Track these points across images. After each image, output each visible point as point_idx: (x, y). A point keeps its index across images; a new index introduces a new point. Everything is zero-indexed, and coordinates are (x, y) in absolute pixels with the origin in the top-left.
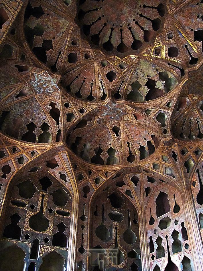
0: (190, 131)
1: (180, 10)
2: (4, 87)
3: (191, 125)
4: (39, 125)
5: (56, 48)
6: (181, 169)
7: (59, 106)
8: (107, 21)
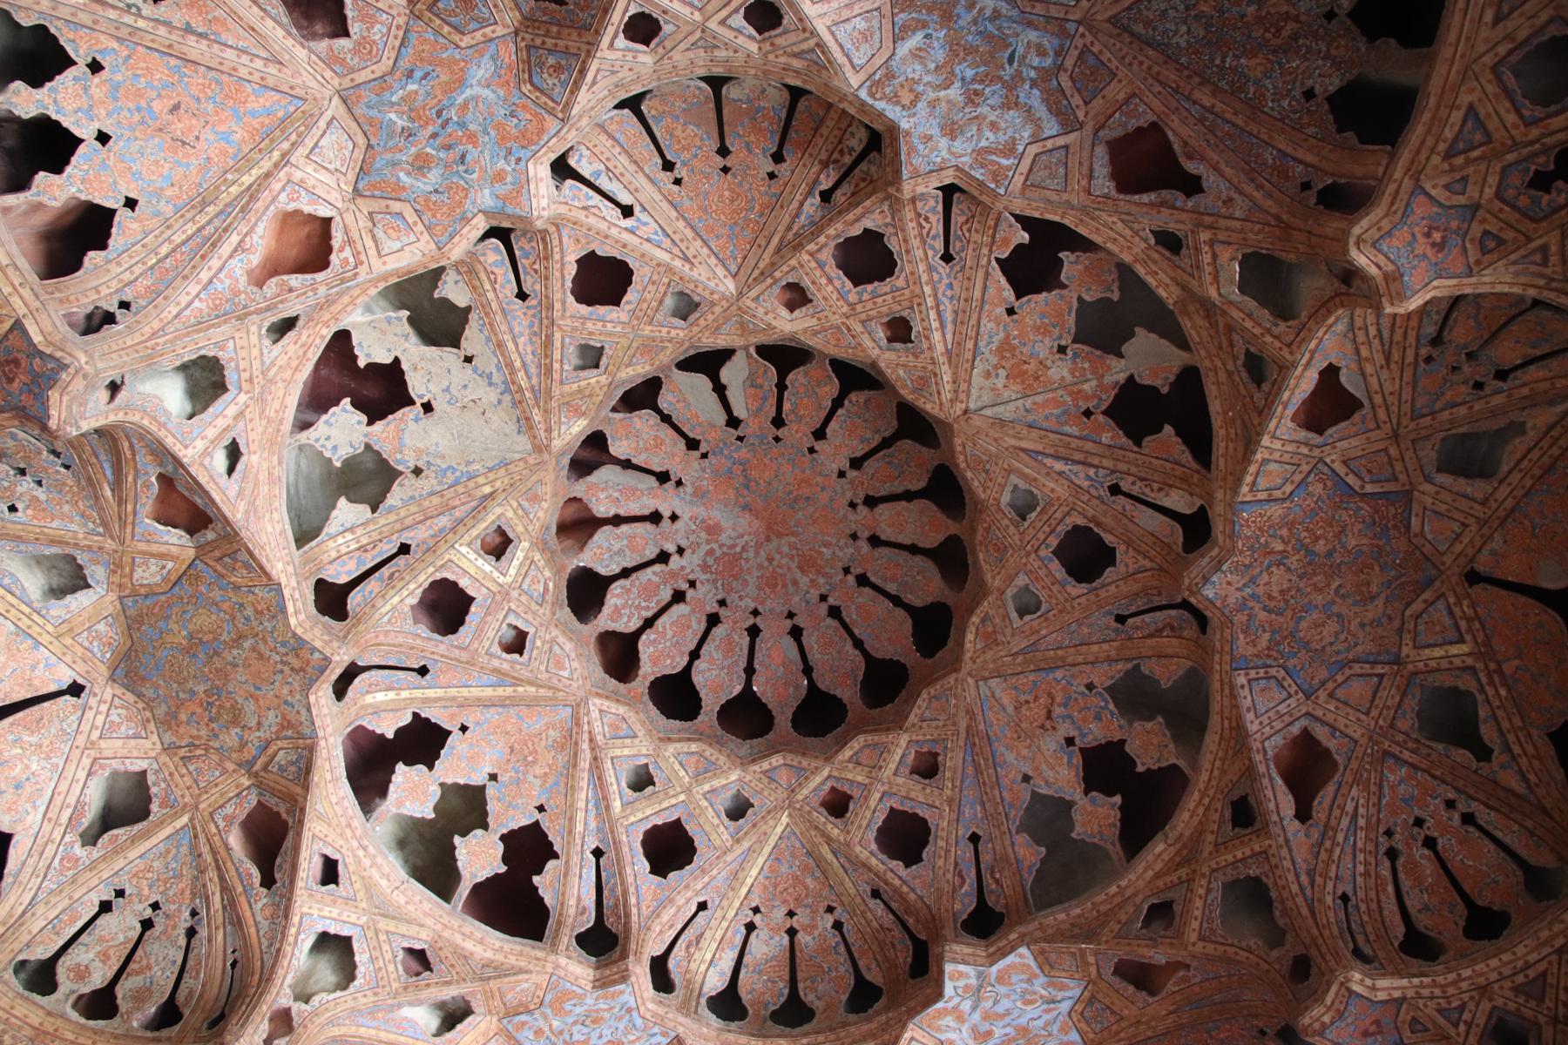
1: (576, 744)
5: (981, 274)
8: (777, 439)
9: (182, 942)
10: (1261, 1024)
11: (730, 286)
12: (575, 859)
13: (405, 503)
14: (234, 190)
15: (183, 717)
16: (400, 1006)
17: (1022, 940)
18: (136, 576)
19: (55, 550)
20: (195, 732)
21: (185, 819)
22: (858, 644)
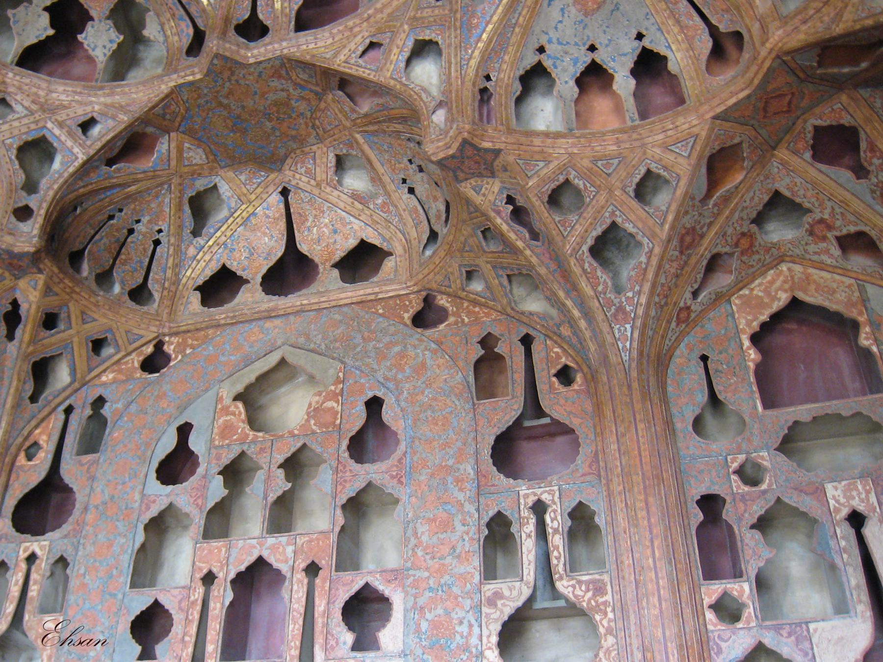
0: (115, 260)
3: (129, 240)
6: (15, 377)
15: (294, 133)
18: (200, 162)
19: (187, 209)
20: (303, 126)
21: (358, 136)
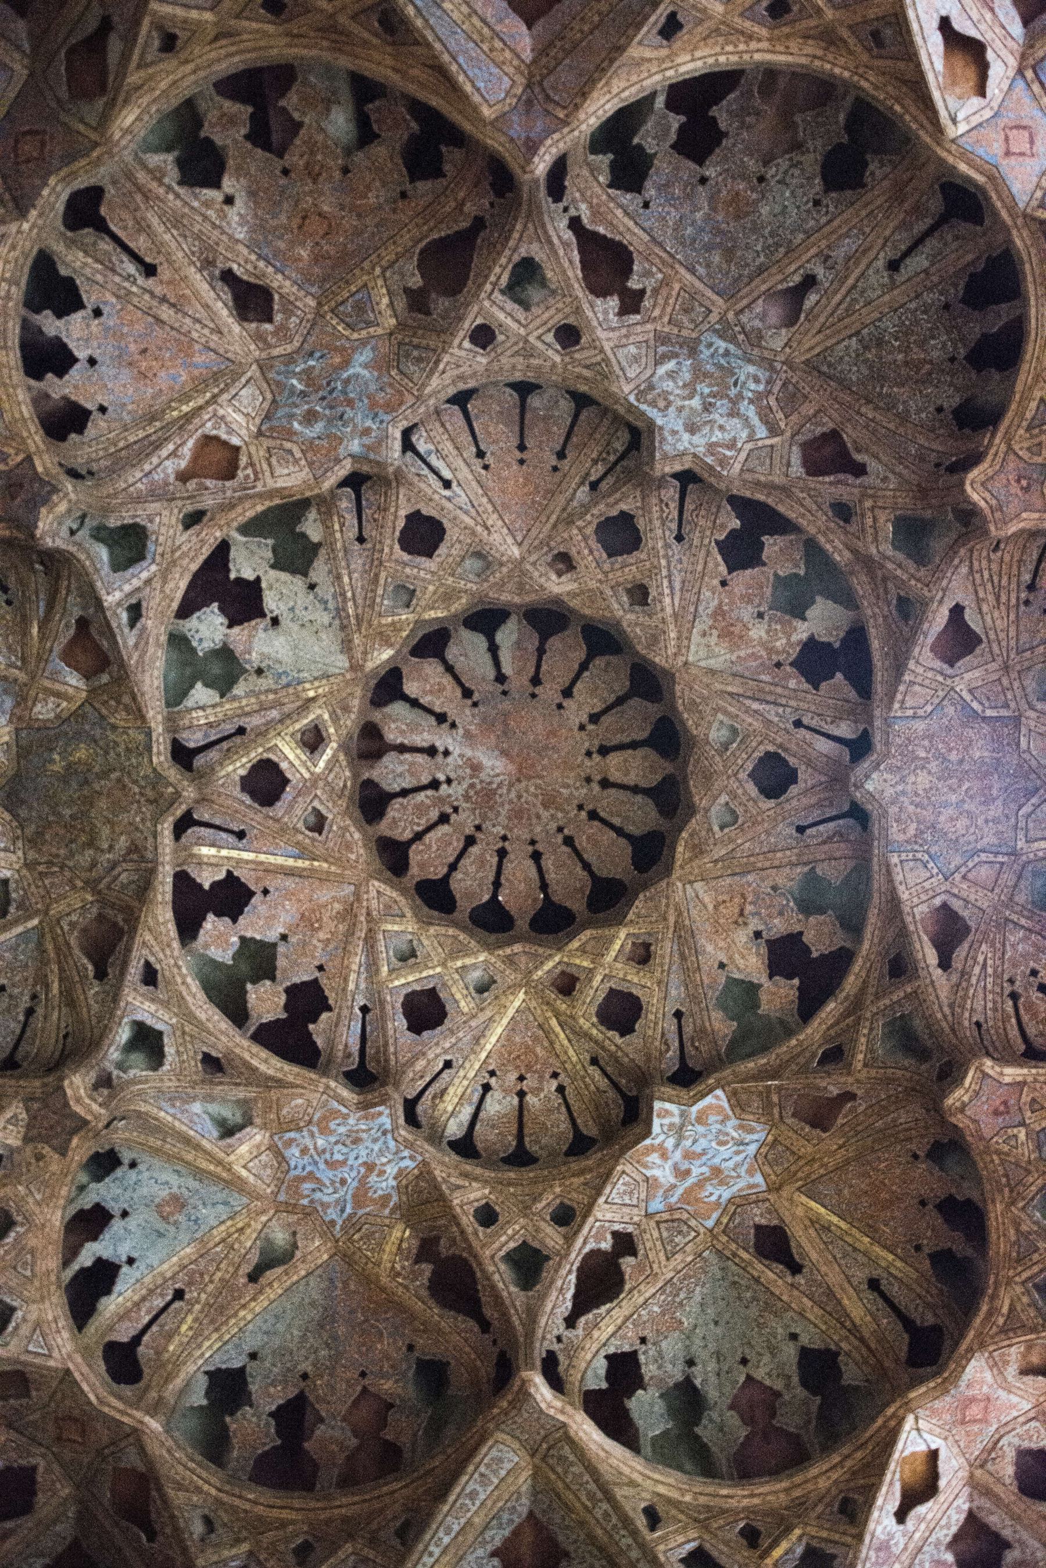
2: (880, 320)
4: (666, 166)
5: (703, 553)
7: (601, 313)
8: (534, 696)
9: (21, 1018)
10: (913, 1147)
11: (516, 552)
12: (345, 1012)
13: (247, 695)
14: (175, 413)
15: (47, 837)
16: (194, 1099)
17: (719, 1085)
18: (36, 710)
20: (54, 850)
21: (35, 922)
22: (586, 866)
